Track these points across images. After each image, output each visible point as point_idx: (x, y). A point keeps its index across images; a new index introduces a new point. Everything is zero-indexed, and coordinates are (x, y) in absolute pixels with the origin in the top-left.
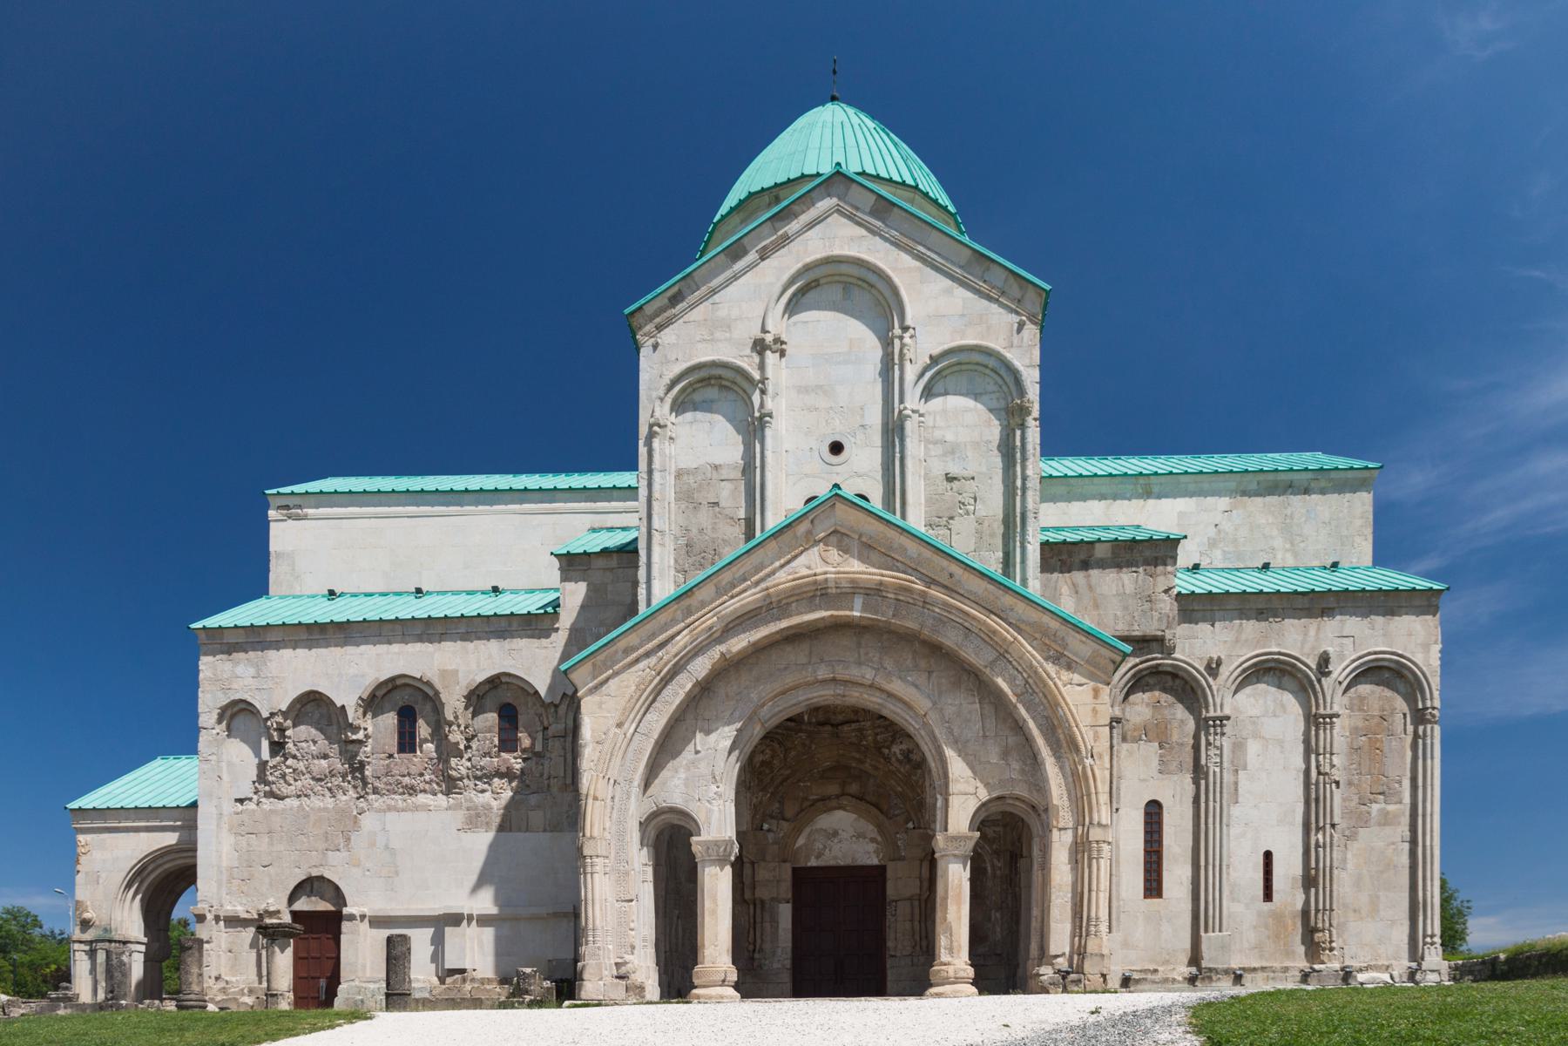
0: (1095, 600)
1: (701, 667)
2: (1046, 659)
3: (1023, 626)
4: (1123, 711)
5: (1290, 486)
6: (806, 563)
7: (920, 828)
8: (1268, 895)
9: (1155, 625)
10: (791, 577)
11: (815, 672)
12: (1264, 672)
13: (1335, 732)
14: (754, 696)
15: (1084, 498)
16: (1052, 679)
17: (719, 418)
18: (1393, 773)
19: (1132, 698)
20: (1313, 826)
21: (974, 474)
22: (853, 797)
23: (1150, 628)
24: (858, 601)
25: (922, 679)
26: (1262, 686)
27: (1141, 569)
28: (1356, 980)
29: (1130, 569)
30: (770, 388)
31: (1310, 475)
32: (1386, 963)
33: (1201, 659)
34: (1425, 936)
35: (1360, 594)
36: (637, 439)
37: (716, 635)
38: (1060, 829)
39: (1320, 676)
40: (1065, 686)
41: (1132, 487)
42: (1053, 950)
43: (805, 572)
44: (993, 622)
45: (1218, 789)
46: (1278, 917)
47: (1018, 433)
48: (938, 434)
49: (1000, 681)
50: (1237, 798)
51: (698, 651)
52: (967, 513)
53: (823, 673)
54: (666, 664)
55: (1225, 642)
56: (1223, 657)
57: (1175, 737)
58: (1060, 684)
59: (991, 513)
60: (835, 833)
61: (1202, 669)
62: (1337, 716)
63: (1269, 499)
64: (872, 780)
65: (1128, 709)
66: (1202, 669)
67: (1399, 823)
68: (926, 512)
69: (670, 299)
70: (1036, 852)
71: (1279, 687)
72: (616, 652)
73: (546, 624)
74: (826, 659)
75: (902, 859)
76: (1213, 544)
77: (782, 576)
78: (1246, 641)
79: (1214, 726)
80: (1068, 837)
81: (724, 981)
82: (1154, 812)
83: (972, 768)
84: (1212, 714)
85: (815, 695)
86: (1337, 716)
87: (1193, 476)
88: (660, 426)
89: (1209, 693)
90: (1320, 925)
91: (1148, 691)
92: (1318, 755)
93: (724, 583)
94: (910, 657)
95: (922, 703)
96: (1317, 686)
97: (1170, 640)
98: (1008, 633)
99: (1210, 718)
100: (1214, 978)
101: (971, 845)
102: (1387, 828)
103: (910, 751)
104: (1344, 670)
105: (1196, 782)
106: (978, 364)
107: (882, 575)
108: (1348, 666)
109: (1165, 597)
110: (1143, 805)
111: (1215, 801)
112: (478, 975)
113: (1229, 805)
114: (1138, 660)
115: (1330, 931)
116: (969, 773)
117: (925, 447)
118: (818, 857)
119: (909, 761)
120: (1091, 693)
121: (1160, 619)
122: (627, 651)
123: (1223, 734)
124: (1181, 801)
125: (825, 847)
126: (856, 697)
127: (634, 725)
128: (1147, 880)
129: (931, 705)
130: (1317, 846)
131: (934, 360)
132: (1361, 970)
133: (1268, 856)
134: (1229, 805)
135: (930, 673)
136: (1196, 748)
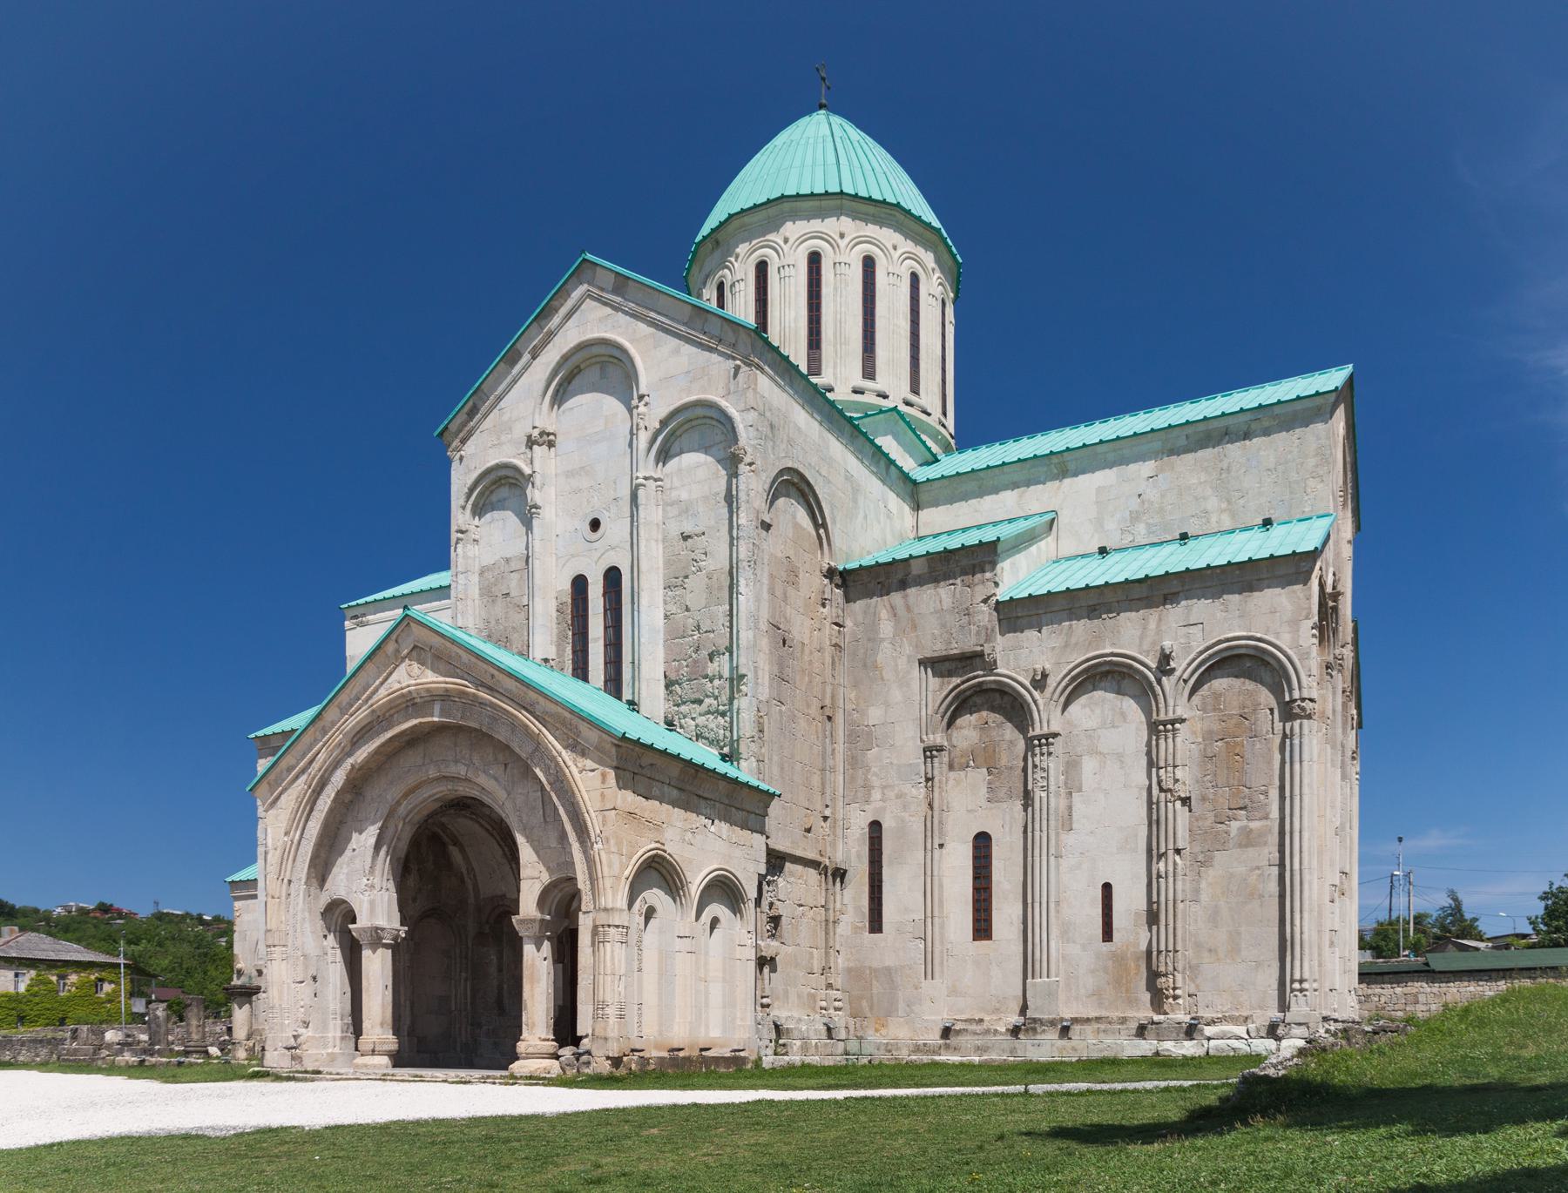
0: (913, 620)
1: (339, 778)
2: (565, 748)
3: (546, 718)
4: (949, 740)
5: (1226, 434)
6: (397, 678)
9: (973, 640)
10: (387, 693)
11: (427, 771)
12: (1101, 678)
13: (1179, 740)
14: (389, 797)
15: (996, 490)
16: (568, 767)
17: (509, 513)
18: (1257, 781)
19: (959, 722)
20: (1155, 852)
21: (704, 529)
23: (968, 644)
26: (1098, 694)
27: (958, 581)
28: (1202, 1034)
29: (947, 582)
30: (538, 479)
31: (1249, 416)
32: (1245, 1014)
33: (1027, 671)
34: (1292, 981)
35: (1209, 572)
36: (450, 546)
37: (347, 749)
38: (585, 913)
39: (1160, 675)
40: (580, 772)
41: (1045, 469)
43: (397, 686)
44: (524, 717)
45: (1045, 816)
47: (734, 481)
48: (674, 494)
49: (538, 771)
50: (1071, 824)
51: (336, 764)
52: (700, 570)
53: (433, 773)
54: (314, 778)
56: (1048, 666)
57: (1004, 761)
58: (574, 770)
59: (719, 566)
61: (1027, 683)
62: (1182, 721)
63: (1200, 453)
65: (955, 734)
66: (1027, 683)
67: (1265, 843)
68: (665, 575)
69: (468, 414)
71: (1118, 693)
72: (282, 772)
76: (1135, 517)
77: (382, 692)
78: (1076, 644)
79: (1040, 745)
81: (373, 1051)
83: (537, 853)
84: (1038, 732)
85: (435, 791)
86: (1182, 721)
87: (1111, 444)
88: (462, 532)
89: (1034, 708)
90: (1162, 969)
91: (975, 712)
92: (1159, 768)
93: (344, 704)
96: (1158, 688)
97: (989, 655)
98: (535, 726)
99: (1034, 737)
102: (1250, 849)
104: (1189, 665)
106: (705, 417)
107: (446, 683)
108: (1194, 660)
109: (984, 607)
111: (1041, 831)
113: (1057, 834)
114: (959, 680)
115: (1174, 975)
116: (535, 858)
117: (663, 510)
120: (600, 778)
121: (978, 633)
122: (290, 770)
123: (1050, 754)
124: (1011, 828)
126: (463, 790)
127: (298, 833)
128: (976, 920)
129: (506, 796)
130: (1159, 876)
131: (664, 423)
132: (1212, 1022)
134: (1057, 834)
136: (1025, 770)
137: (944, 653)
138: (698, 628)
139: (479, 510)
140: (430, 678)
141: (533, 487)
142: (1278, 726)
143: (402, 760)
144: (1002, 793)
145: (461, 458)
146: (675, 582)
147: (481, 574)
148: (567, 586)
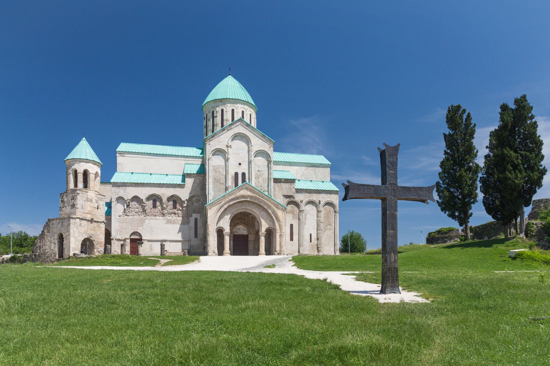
1: (226, 206)
8: (311, 241)
14: (233, 210)
24: (249, 198)
25: (258, 209)
42: (277, 250)
44: (268, 202)
46: (312, 245)
53: (243, 207)
57: (295, 213)
60: (240, 229)
70: (274, 235)
73: (183, 186)
80: (279, 234)
82: (292, 226)
95: (258, 213)
105: (299, 221)
112: (169, 252)
118: (237, 233)
119: (252, 218)
122: (215, 204)
126: (248, 211)
133: (311, 234)
138: (261, 186)
139: (213, 155)
140: (249, 193)
141: (228, 154)
142: (334, 214)
144: (295, 218)
145: (209, 144)
146: (257, 178)
147: (213, 166)
148: (234, 173)
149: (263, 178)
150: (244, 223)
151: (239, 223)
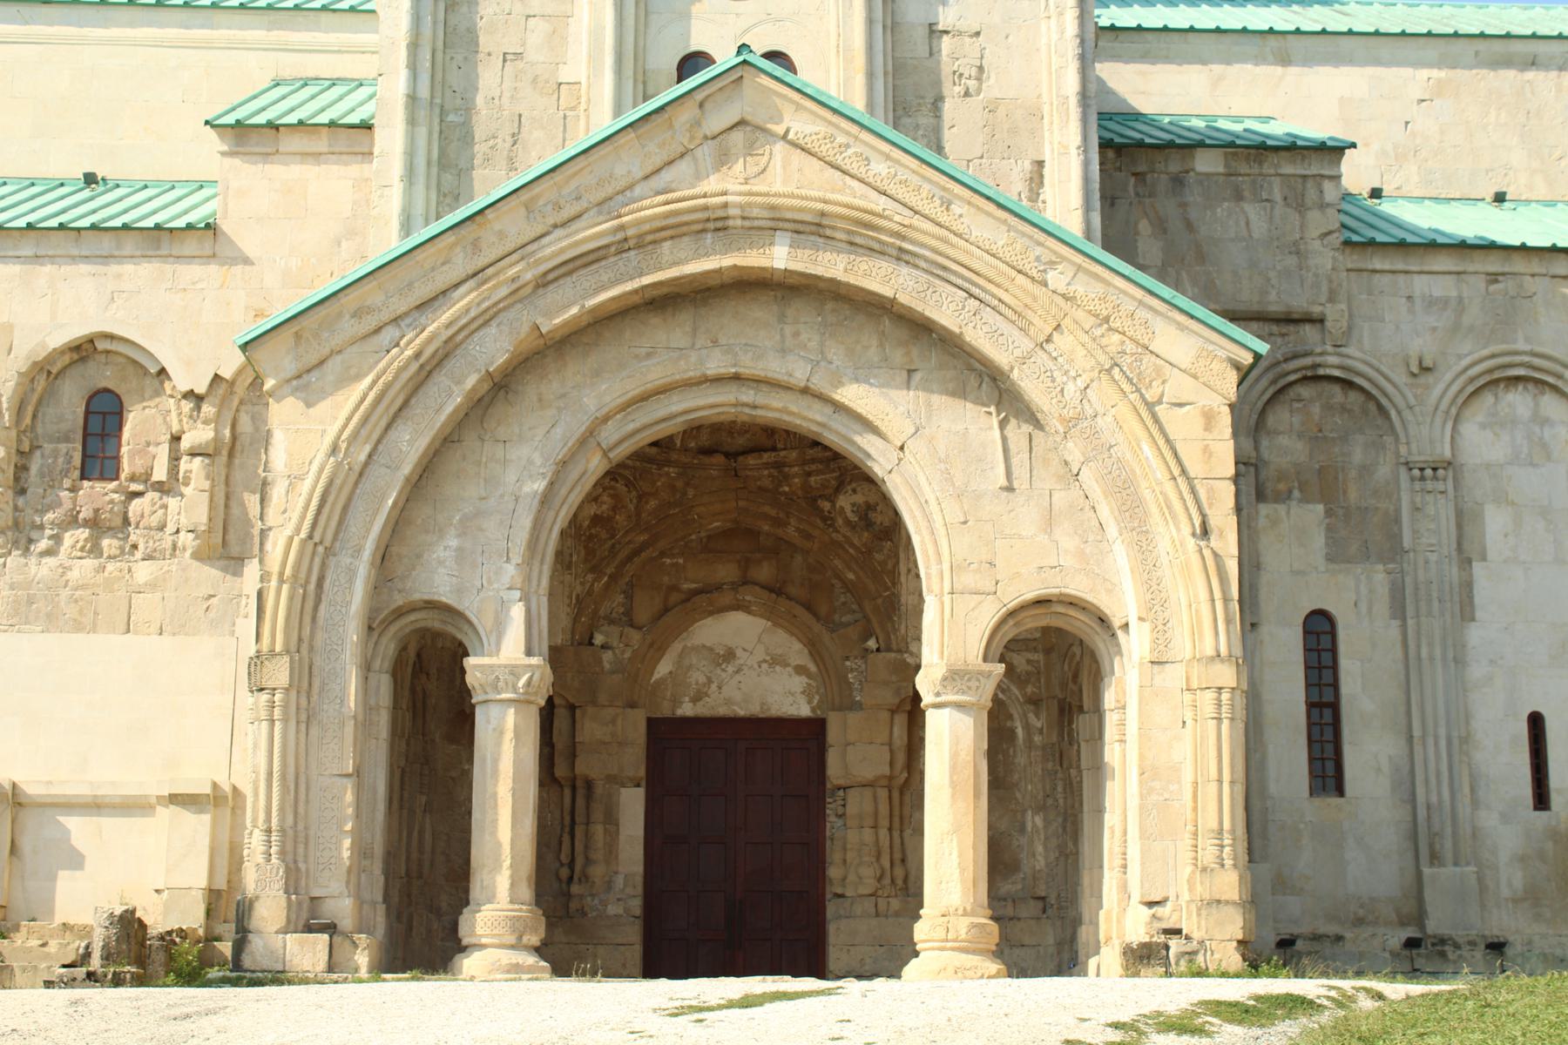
7: (889, 650)
22: (763, 587)
23: (1299, 302)
53: (716, 365)
55: (1434, 329)
64: (799, 558)
74: (723, 341)
75: (854, 706)
94: (875, 342)
100: (1451, 956)
101: (989, 687)
103: (870, 507)
110: (1301, 621)
118: (695, 700)
125: (710, 681)
135: (910, 372)
137: (1255, 307)
143: (628, 334)
149: (991, 108)
150: (776, 590)
151: (718, 588)
